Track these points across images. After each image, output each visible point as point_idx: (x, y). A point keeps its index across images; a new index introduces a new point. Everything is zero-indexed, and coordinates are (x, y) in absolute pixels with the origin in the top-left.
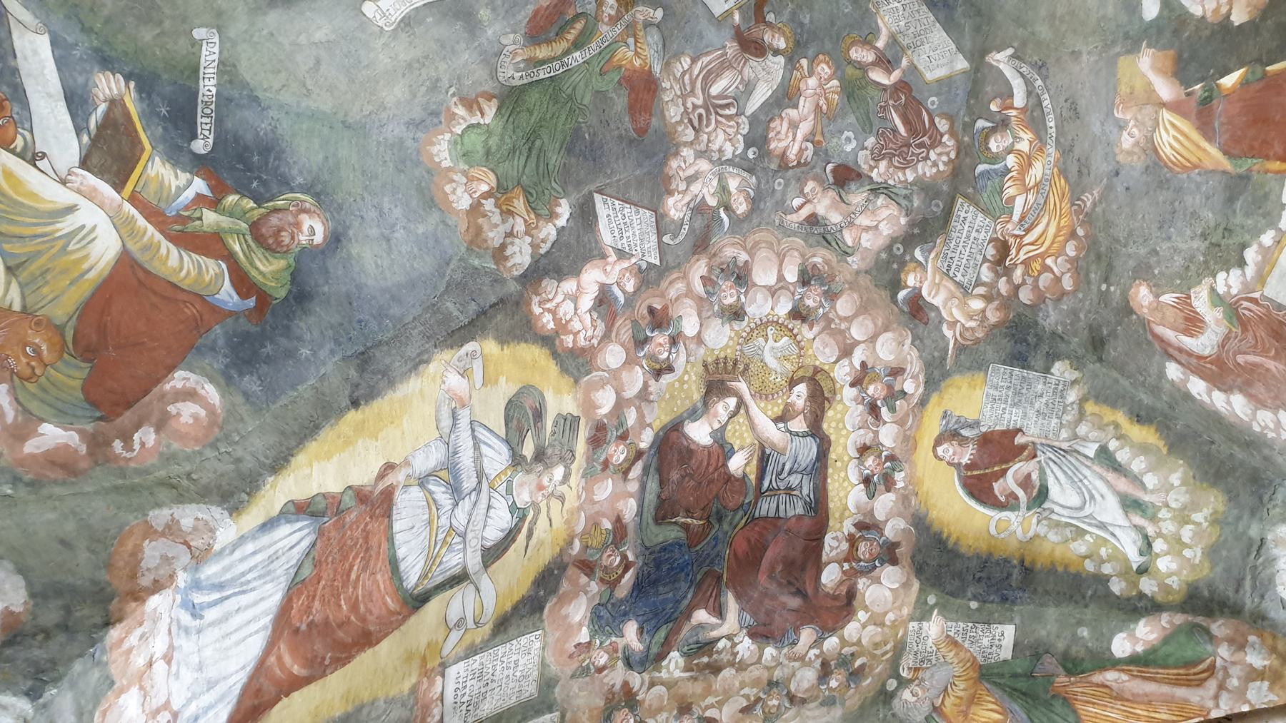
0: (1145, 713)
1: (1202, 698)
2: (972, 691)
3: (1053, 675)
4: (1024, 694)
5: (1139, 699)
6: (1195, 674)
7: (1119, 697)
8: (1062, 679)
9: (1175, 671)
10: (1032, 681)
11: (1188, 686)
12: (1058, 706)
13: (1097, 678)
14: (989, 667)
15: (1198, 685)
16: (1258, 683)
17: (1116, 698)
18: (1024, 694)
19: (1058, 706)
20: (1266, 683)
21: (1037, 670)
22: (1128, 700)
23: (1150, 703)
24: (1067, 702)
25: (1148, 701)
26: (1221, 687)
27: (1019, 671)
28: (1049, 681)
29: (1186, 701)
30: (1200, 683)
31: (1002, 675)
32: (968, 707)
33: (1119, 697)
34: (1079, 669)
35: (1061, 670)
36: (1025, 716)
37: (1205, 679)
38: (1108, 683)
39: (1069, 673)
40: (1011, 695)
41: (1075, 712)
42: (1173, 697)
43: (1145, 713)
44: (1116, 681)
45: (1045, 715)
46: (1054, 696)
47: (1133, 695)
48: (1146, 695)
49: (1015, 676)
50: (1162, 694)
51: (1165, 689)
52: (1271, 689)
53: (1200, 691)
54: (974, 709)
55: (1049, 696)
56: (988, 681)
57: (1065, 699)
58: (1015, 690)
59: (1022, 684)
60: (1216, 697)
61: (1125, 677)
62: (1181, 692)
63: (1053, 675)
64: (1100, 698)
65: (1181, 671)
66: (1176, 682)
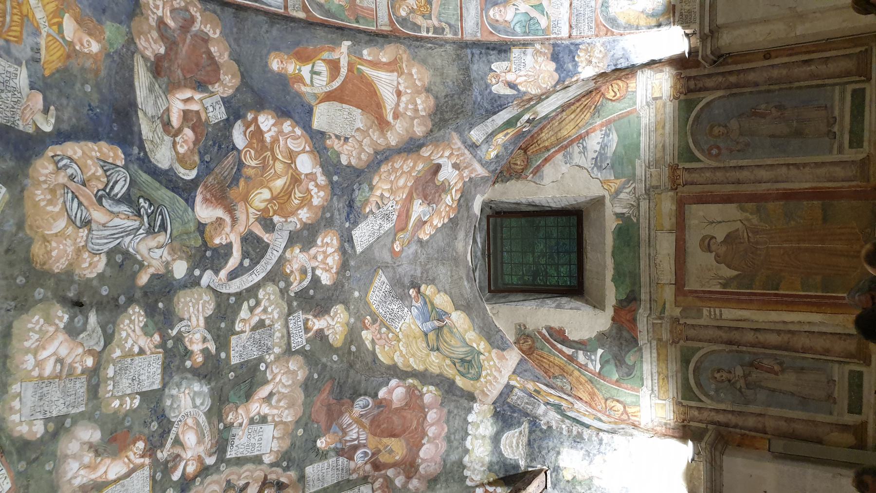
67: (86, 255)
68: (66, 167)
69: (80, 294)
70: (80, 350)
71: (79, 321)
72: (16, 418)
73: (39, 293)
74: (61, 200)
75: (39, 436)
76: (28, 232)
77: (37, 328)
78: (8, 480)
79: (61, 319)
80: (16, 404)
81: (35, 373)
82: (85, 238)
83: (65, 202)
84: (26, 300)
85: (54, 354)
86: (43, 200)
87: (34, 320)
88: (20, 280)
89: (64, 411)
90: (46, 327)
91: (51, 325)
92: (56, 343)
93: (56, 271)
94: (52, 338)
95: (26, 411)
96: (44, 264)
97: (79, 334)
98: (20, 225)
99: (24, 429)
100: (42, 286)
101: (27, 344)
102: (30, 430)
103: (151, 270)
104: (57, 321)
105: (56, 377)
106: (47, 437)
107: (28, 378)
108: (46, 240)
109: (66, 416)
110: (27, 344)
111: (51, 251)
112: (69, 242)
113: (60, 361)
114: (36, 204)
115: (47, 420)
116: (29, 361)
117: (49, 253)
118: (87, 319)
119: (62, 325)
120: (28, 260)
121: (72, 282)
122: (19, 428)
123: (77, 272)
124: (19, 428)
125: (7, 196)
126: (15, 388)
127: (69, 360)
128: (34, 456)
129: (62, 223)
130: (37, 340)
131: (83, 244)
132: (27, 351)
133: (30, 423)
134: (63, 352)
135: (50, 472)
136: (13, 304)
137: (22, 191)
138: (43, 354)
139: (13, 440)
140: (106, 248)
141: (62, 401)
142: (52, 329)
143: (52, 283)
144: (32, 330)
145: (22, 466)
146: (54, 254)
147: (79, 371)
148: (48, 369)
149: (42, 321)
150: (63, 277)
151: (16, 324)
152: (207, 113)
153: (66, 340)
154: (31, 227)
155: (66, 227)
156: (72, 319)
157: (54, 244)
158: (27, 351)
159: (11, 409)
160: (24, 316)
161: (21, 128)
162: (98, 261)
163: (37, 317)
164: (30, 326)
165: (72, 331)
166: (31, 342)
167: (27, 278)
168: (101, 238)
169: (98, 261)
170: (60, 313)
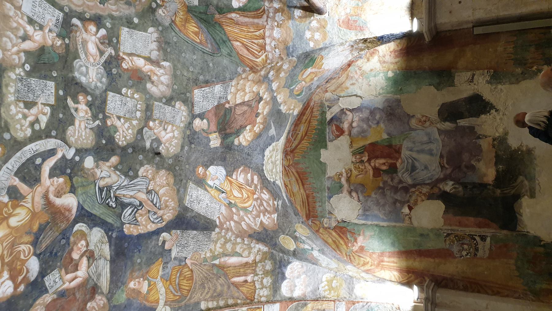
0: (246, 30)
1: (263, 22)
2: (186, 16)
3: (214, 14)
4: (205, 21)
5: (243, 24)
6: (259, 13)
7: (237, 24)
8: (217, 16)
9: (253, 13)
10: (207, 16)
11: (258, 18)
12: (217, 26)
13: (229, 16)
14: (191, 7)
15: (261, 17)
16: (278, 14)
17: (236, 24)
18: (205, 21)
19: (217, 26)
20: (280, 13)
21: (208, 11)
22: (240, 25)
23: (247, 26)
24: (220, 25)
25: (246, 25)
26: (268, 17)
27: (202, 11)
28: (213, 16)
29: (258, 24)
30: (261, 17)
31: (196, 12)
32: (185, 23)
33: (237, 24)
34: (223, 12)
35: (216, 12)
36: (206, 31)
37: (263, 15)
38: (233, 18)
39: (220, 13)
40: (200, 21)
41: (223, 29)
42: (254, 23)
43: (246, 30)
44: (235, 17)
45: (213, 30)
46: (215, 23)
47: (241, 23)
48: (246, 22)
49: (200, 13)
50: (250, 22)
51: (251, 20)
52: (282, 15)
53: (262, 20)
54: (187, 25)
55: (214, 23)
56: (191, 13)
57: (219, 24)
58: (201, 19)
59: (203, 16)
60: (267, 21)
61: (238, 16)
62: (256, 21)
63: (214, 14)
64: (231, 24)
65: (255, 13)
66: (254, 17)
67: (150, 176)
68: (157, 218)
69: (153, 158)
70: (155, 131)
71: (155, 145)
72: (184, 114)
73: (170, 161)
74: (162, 202)
75: (178, 102)
76: (175, 188)
77: (172, 147)
78: (195, 93)
79: (163, 148)
80: (183, 119)
81: (174, 128)
82: (150, 185)
83: (160, 202)
84: (175, 159)
85: (167, 133)
86: (170, 202)
87: (173, 150)
88: (177, 168)
89: (166, 106)
90: (169, 146)
91: (167, 147)
92: (166, 138)
93: (164, 170)
94: (167, 140)
95: (180, 114)
96: (169, 174)
97: (155, 139)
98: (178, 191)
99: (183, 108)
100: (169, 164)
101: (176, 141)
102: (181, 106)
103: (108, 164)
104: (164, 147)
105: (167, 123)
106: (176, 99)
107: (178, 127)
108: (168, 184)
109: (165, 104)
110: (176, 141)
111: (166, 179)
112: (158, 183)
113: (165, 130)
114: (173, 200)
115: (174, 106)
116: (176, 133)
117: (167, 179)
118: (151, 145)
119: (163, 145)
120: (175, 176)
121: (157, 164)
122: (184, 109)
123: (154, 169)
124: (184, 109)
125: (184, 202)
126: (182, 125)
127: (161, 128)
128: (183, 95)
129: (161, 192)
130: (173, 141)
131: (151, 182)
132: (176, 138)
133: (180, 109)
134: (163, 133)
135: (175, 84)
136: (180, 159)
137: (179, 205)
138: (171, 135)
139: (188, 105)
140: (139, 179)
141: (166, 111)
142: (167, 145)
143: (166, 165)
144: (175, 147)
145: (188, 95)
146: (165, 178)
147: (157, 122)
148: (170, 127)
149: (170, 149)
150: (161, 167)
151: (179, 150)
152: (60, 276)
153: (162, 138)
154: (174, 190)
155: (159, 190)
156: (158, 147)
157: (165, 182)
158: (176, 138)
159: (185, 118)
160: (176, 153)
161: (178, 231)
162: (143, 173)
163: (172, 151)
164: (174, 148)
165: (158, 141)
166: (175, 142)
167: (175, 169)
168: (141, 184)
169: (143, 173)
170: (163, 151)
